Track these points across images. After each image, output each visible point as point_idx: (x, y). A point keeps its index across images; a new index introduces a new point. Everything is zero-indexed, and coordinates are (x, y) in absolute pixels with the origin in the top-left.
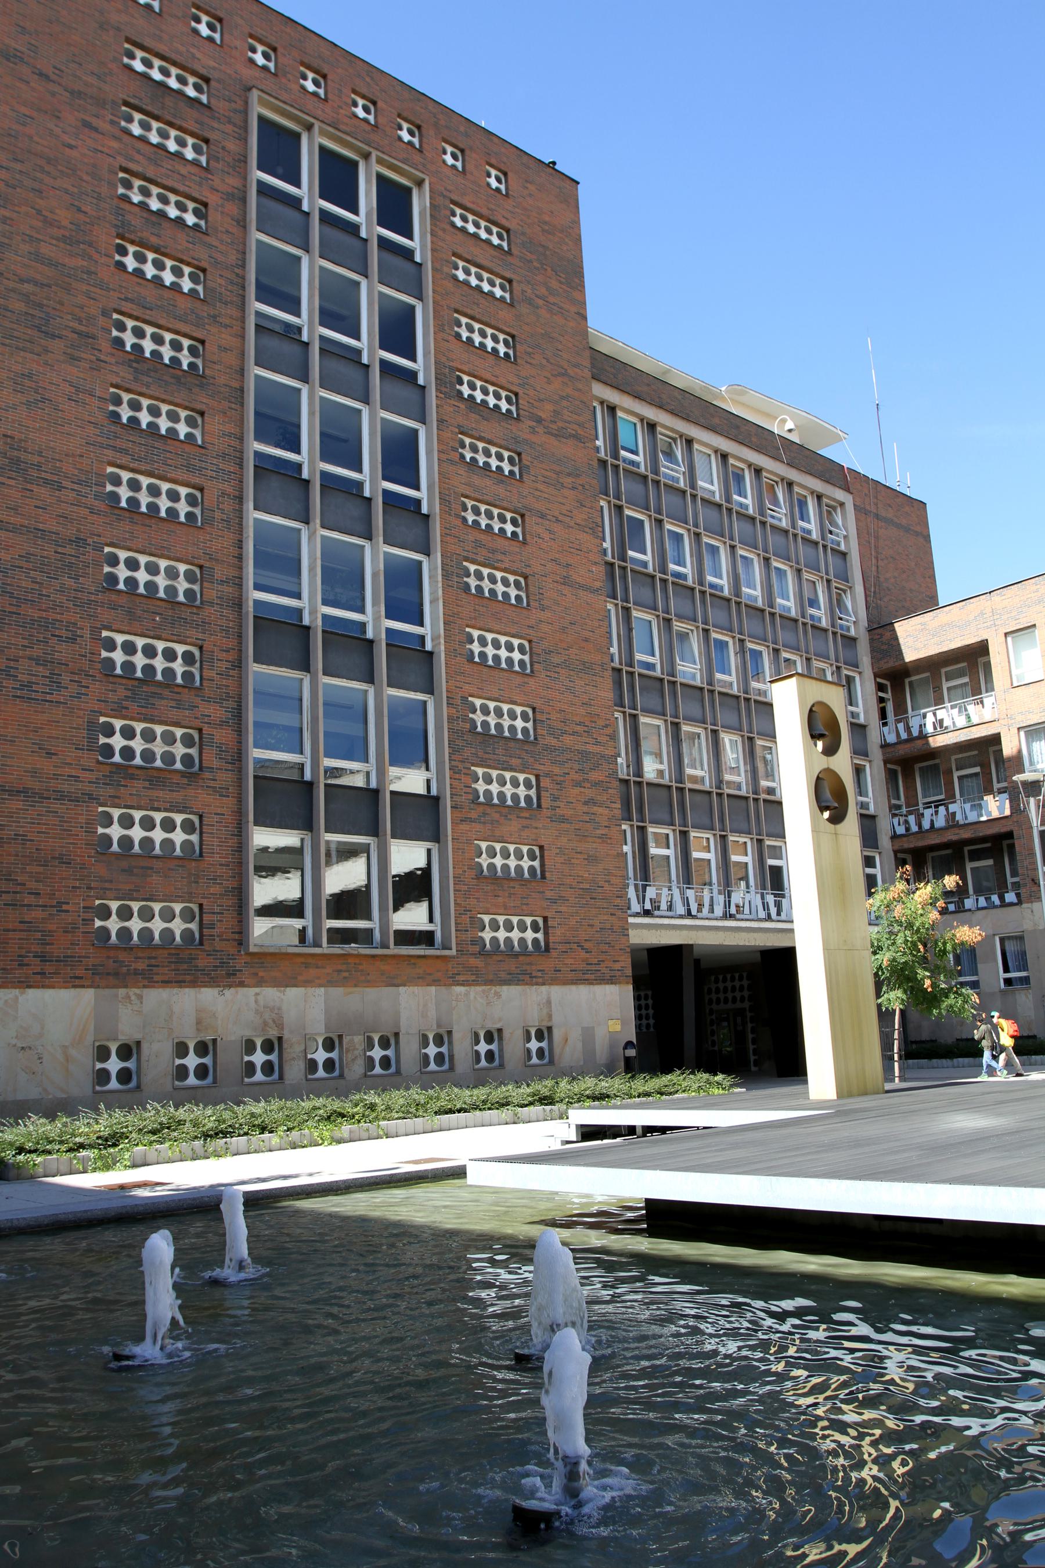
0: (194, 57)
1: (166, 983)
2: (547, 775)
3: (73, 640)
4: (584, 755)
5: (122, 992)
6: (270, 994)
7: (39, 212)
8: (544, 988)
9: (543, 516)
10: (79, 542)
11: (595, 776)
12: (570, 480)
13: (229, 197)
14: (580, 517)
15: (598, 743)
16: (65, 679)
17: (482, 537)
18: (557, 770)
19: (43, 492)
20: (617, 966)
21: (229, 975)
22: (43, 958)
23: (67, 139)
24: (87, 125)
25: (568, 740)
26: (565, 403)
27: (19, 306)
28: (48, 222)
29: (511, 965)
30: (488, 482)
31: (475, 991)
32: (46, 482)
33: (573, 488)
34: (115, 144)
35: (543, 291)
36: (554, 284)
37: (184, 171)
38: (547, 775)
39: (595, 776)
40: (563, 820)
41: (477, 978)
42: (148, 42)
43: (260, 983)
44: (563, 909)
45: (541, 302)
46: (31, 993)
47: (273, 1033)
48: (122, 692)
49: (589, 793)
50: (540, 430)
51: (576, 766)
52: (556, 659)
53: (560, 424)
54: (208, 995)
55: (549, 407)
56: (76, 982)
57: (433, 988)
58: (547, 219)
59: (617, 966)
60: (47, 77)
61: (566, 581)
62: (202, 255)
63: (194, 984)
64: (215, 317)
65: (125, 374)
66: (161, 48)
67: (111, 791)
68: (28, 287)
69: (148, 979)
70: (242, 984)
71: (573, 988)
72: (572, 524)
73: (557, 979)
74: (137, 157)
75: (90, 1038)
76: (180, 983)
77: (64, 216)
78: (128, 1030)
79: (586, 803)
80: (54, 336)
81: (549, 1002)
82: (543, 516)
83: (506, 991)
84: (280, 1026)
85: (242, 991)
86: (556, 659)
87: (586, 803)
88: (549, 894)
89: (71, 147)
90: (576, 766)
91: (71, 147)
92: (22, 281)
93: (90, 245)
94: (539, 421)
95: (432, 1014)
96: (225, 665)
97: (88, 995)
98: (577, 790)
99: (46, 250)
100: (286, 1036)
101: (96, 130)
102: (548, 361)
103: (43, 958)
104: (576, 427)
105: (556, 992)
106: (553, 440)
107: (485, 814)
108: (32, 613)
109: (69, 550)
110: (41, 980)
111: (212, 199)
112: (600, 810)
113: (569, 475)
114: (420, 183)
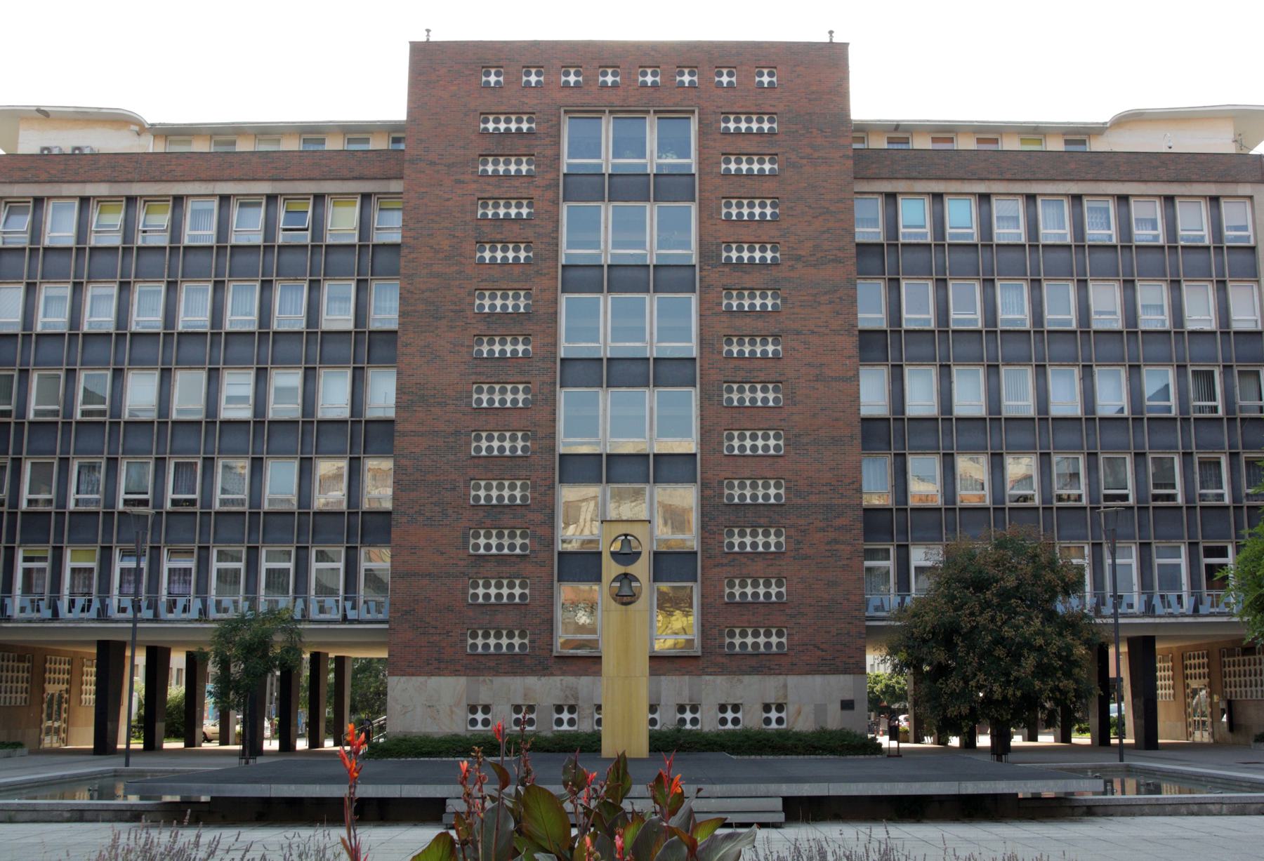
0: (524, 103)
1: (506, 674)
2: (791, 526)
3: (454, 489)
5: (481, 678)
6: (570, 680)
7: (431, 247)
8: (781, 678)
9: (798, 333)
10: (457, 433)
11: (838, 522)
12: (827, 297)
13: (548, 187)
15: (842, 496)
16: (450, 511)
17: (737, 363)
18: (802, 522)
20: (852, 661)
21: (544, 669)
22: (439, 661)
23: (446, 196)
24: (458, 182)
25: (813, 499)
26: (826, 236)
30: (748, 320)
31: (720, 679)
32: (439, 404)
33: (830, 303)
34: (474, 186)
35: (809, 151)
37: (516, 183)
38: (791, 526)
39: (838, 522)
40: (806, 557)
41: (723, 670)
42: (494, 109)
43: (564, 674)
44: (801, 621)
45: (804, 161)
46: (434, 679)
47: (572, 702)
48: (481, 514)
50: (799, 265)
51: (821, 517)
52: (805, 440)
53: (819, 255)
54: (531, 681)
56: (456, 673)
57: (687, 678)
58: (814, 88)
59: (852, 661)
60: (435, 164)
62: (529, 233)
63: (523, 674)
64: (537, 272)
65: (481, 328)
66: (502, 109)
67: (475, 570)
68: (427, 294)
69: (497, 672)
70: (552, 674)
71: (809, 677)
72: (827, 331)
73: (792, 670)
74: (490, 188)
75: (464, 703)
76: (514, 674)
78: (484, 699)
79: (828, 543)
80: (441, 318)
81: (785, 686)
82: (798, 333)
83: (746, 679)
84: (577, 698)
85: (552, 678)
86: (805, 440)
87: (828, 543)
88: (789, 611)
89: (448, 200)
90: (821, 517)
91: (448, 200)
92: (423, 292)
93: (460, 255)
94: (798, 258)
95: (686, 693)
96: (543, 489)
97: (462, 681)
98: (821, 534)
100: (580, 703)
101: (463, 182)
102: (810, 207)
103: (439, 661)
104: (835, 252)
105: (792, 680)
107: (734, 560)
109: (451, 439)
110: (438, 672)
111: (535, 193)
112: (843, 547)
113: (826, 293)
114: (693, 112)
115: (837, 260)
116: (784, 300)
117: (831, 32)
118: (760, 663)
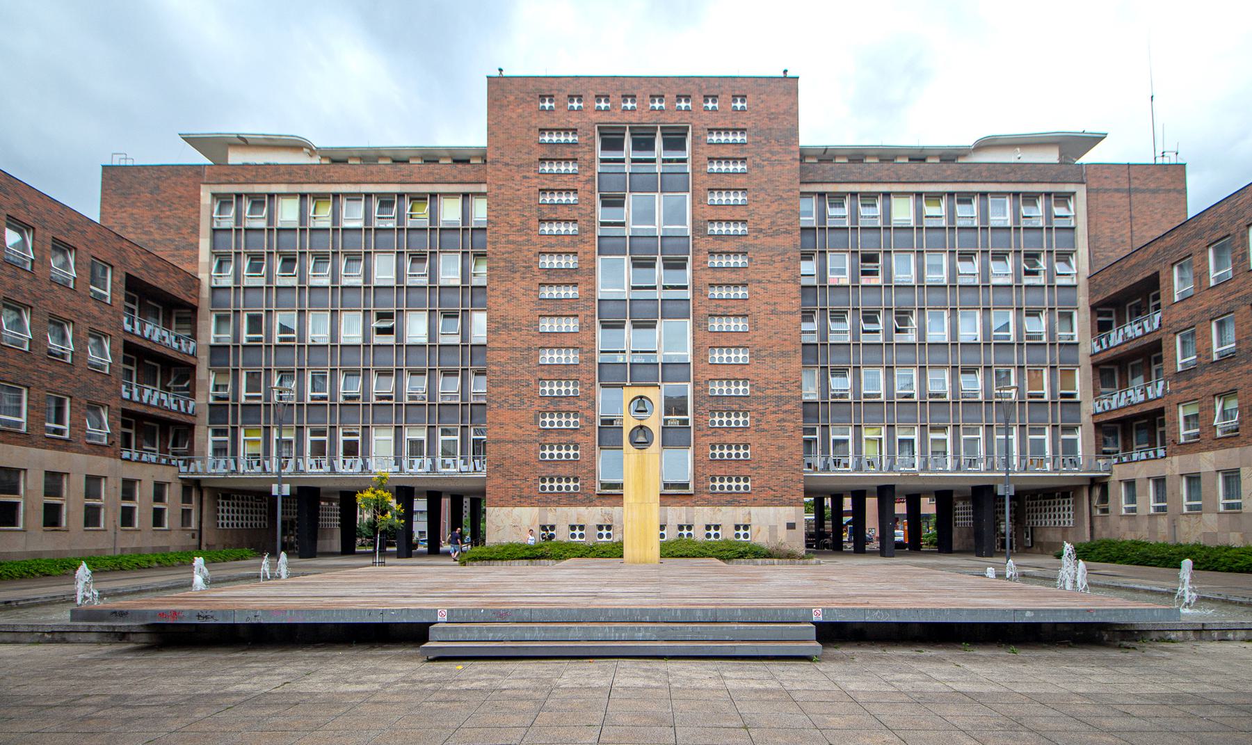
4: (780, 398)
9: (760, 282)
14: (785, 276)
18: (761, 407)
19: (515, 334)
24: (525, 177)
25: (769, 392)
27: (502, 264)
28: (512, 226)
29: (728, 498)
35: (768, 155)
36: (776, 148)
40: (763, 430)
49: (781, 416)
50: (761, 236)
52: (763, 353)
55: (768, 221)
61: (773, 312)
73: (755, 503)
77: (517, 221)
82: (760, 282)
86: (763, 353)
94: (761, 231)
99: (511, 238)
105: (754, 510)
106: (769, 239)
108: (513, 378)
115: (787, 232)
116: (750, 260)
117: (785, 72)
118: (734, 499)
